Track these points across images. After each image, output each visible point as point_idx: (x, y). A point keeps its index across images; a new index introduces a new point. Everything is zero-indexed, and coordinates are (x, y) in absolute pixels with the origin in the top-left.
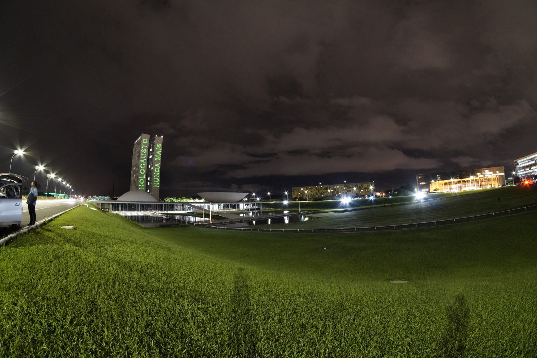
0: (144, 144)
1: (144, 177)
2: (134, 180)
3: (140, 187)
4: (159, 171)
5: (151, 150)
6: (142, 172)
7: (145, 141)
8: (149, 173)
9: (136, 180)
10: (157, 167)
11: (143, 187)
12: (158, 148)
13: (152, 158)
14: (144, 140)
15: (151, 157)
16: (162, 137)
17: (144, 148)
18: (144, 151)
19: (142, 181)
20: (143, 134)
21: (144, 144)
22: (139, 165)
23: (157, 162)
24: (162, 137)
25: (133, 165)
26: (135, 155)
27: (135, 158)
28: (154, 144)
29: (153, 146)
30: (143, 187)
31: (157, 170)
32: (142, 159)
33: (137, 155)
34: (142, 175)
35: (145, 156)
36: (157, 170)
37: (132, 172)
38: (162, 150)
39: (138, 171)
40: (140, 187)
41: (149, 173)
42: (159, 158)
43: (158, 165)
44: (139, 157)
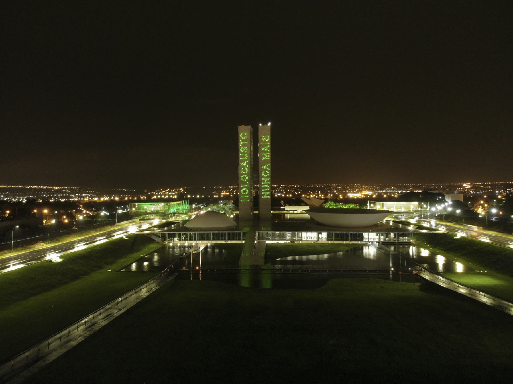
0: (243, 141)
3: (243, 199)
4: (269, 174)
6: (244, 178)
7: (244, 136)
11: (247, 198)
12: (265, 142)
16: (269, 124)
17: (244, 146)
19: (245, 191)
21: (243, 141)
23: (265, 162)
24: (269, 124)
30: (247, 198)
32: (243, 161)
34: (245, 183)
40: (243, 199)
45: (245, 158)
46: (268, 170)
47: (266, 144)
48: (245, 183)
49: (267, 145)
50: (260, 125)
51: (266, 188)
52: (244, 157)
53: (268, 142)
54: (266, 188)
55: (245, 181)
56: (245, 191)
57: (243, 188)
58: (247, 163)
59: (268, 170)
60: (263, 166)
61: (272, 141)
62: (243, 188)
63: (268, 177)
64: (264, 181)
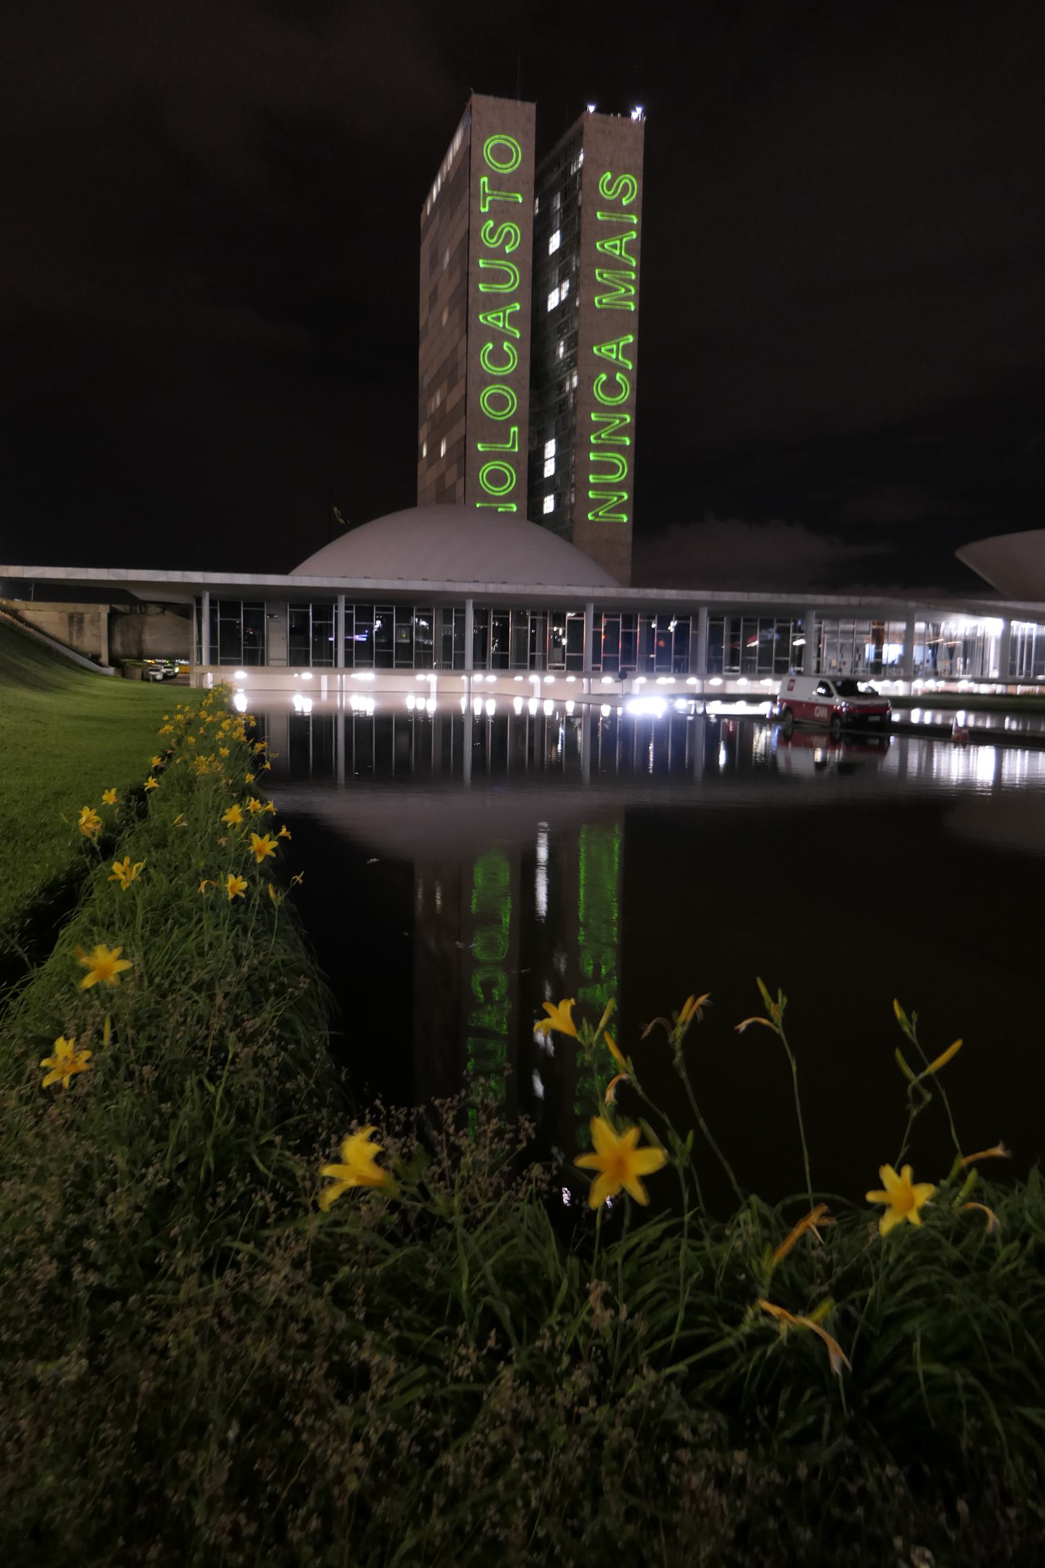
1: (514, 442)
2: (441, 478)
4: (625, 395)
5: (555, 242)
7: (502, 153)
8: (548, 405)
9: (451, 476)
10: (612, 367)
12: (614, 206)
13: (562, 305)
14: (497, 145)
15: (553, 300)
16: (637, 113)
18: (501, 238)
19: (497, 478)
20: (481, 103)
22: (471, 356)
23: (611, 324)
24: (637, 113)
25: (425, 378)
26: (434, 297)
27: (435, 319)
28: (570, 187)
29: (571, 208)
31: (612, 387)
32: (495, 302)
33: (448, 288)
34: (499, 431)
35: (515, 280)
36: (612, 387)
37: (423, 433)
38: (646, 229)
39: (466, 405)
41: (548, 405)
42: (620, 292)
43: (617, 350)
44: (465, 304)
45: (505, 288)
46: (624, 370)
47: (615, 218)
48: (499, 431)
49: (630, 227)
50: (591, 108)
51: (612, 468)
52: (501, 277)
53: (629, 209)
54: (612, 468)
55: (501, 416)
56: (497, 478)
57: (488, 457)
58: (514, 319)
59: (624, 370)
60: (601, 342)
61: (651, 204)
62: (488, 457)
63: (618, 409)
64: (600, 426)
